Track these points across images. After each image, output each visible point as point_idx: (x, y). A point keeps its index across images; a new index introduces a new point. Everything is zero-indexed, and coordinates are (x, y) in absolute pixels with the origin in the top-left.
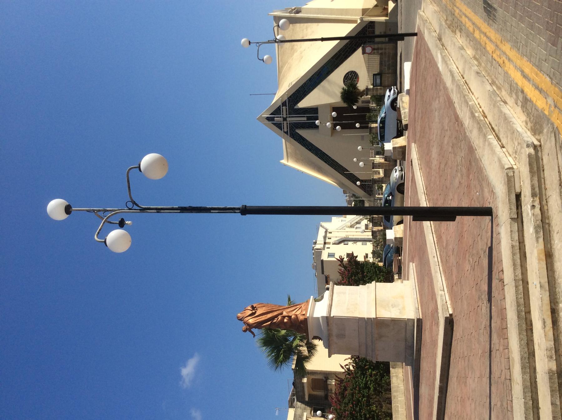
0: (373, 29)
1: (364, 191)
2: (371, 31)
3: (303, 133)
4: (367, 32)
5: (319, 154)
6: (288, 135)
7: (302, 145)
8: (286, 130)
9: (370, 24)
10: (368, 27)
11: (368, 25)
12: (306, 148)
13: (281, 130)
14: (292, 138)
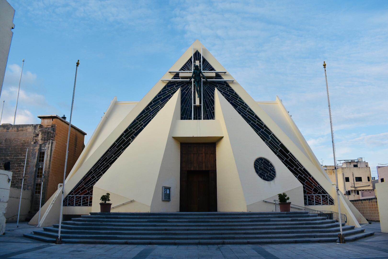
0: (322, 203)
1: (72, 192)
2: (320, 199)
3: (176, 97)
4: (318, 194)
5: (139, 121)
6: (172, 79)
7: (156, 97)
8: (181, 75)
9: (329, 197)
10: (325, 195)
11: (327, 196)
12: (151, 103)
13: (180, 70)
14: (168, 84)
